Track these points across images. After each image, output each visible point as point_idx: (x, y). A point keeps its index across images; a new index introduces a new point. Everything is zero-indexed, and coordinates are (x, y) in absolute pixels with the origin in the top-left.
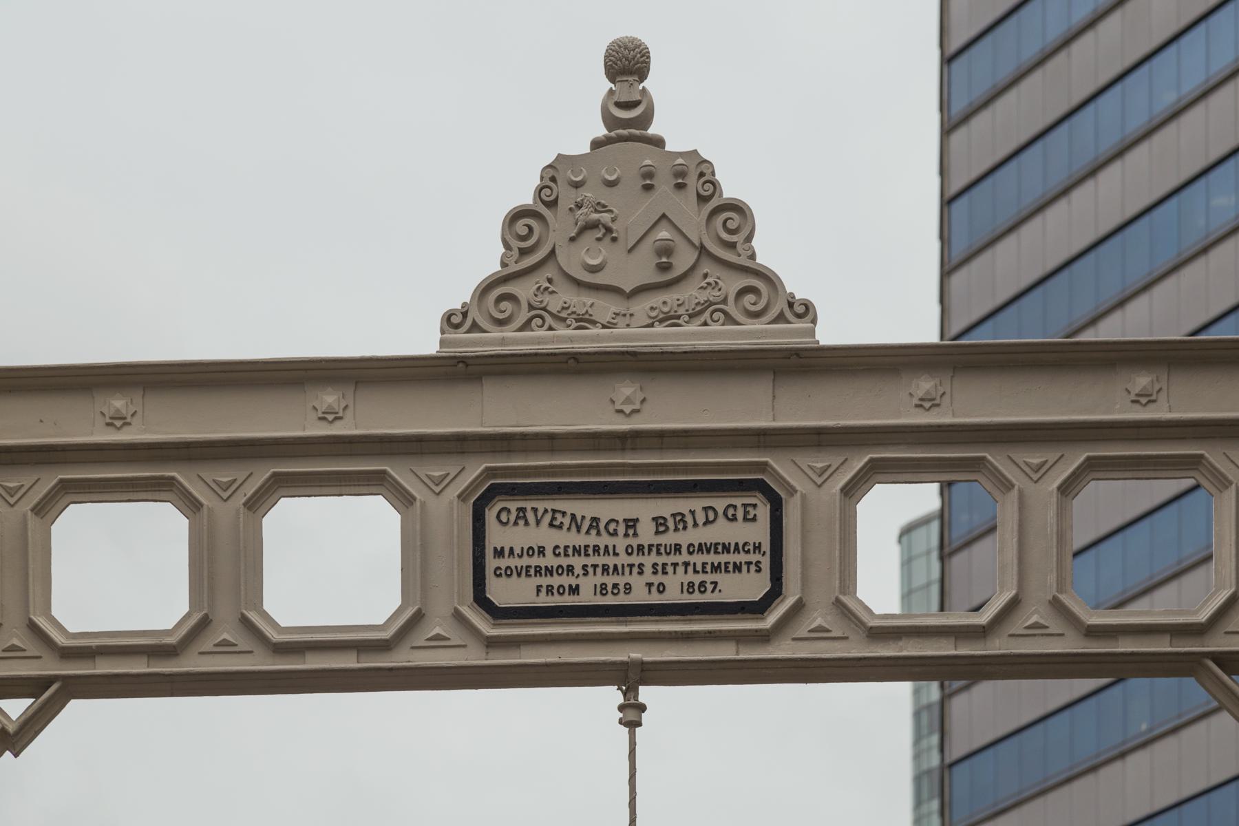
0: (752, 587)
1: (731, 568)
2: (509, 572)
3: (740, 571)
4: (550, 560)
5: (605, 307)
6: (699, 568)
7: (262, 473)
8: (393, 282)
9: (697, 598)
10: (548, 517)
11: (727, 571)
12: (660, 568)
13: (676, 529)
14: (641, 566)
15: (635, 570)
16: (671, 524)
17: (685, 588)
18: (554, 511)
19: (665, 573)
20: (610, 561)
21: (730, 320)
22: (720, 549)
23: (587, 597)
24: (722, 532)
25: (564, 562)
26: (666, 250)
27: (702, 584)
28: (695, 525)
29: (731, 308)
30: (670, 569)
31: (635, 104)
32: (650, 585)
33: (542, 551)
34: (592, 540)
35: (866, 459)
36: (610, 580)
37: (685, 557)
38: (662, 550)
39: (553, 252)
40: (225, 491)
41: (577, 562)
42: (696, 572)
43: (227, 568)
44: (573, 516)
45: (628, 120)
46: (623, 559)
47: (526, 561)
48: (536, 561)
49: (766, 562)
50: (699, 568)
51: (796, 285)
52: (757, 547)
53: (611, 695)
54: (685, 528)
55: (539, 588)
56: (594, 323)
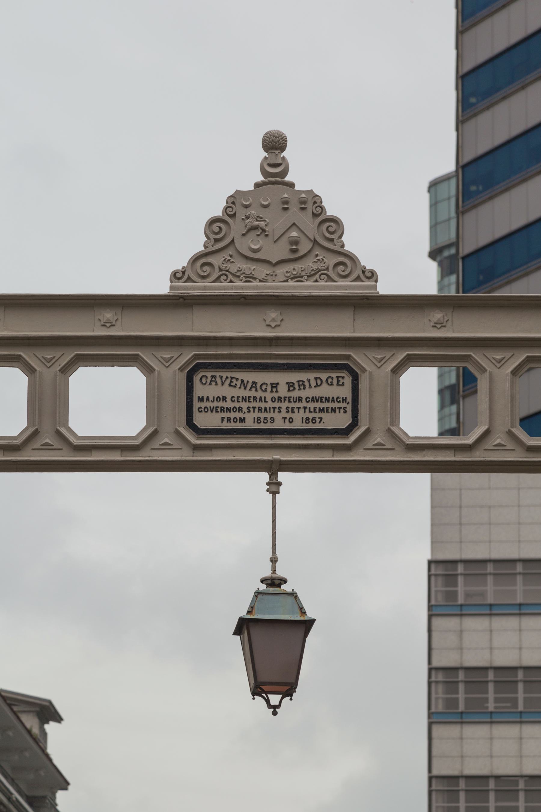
0: (342, 420)
1: (330, 410)
2: (206, 410)
3: (335, 412)
4: (229, 404)
5: (261, 271)
6: (312, 410)
7: (69, 354)
9: (311, 426)
11: (327, 412)
12: (290, 410)
13: (300, 389)
14: (280, 408)
15: (277, 410)
16: (296, 386)
17: (304, 420)
18: (232, 378)
19: (293, 412)
20: (263, 405)
22: (324, 400)
23: (250, 424)
24: (325, 391)
25: (237, 405)
26: (295, 242)
27: (314, 418)
28: (310, 387)
29: (331, 273)
30: (296, 410)
31: (279, 165)
32: (285, 418)
33: (224, 399)
34: (253, 393)
35: (405, 354)
36: (262, 415)
37: (304, 404)
38: (292, 400)
39: (233, 241)
40: (49, 363)
41: (244, 405)
42: (310, 412)
43: (48, 404)
44: (242, 381)
45: (275, 172)
46: (270, 404)
47: (215, 404)
48: (221, 404)
49: (349, 408)
50: (312, 410)
52: (345, 400)
53: (264, 477)
54: (304, 388)
55: (223, 419)
56: (255, 279)
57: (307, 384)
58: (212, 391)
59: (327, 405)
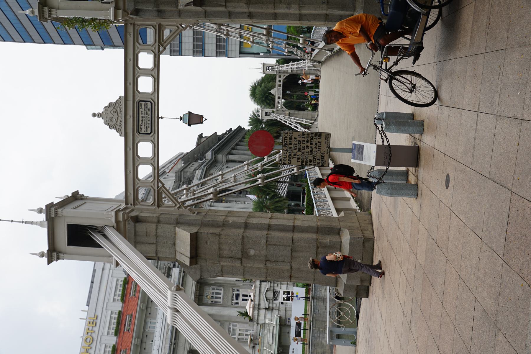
0: (149, 104)
5: (119, 119)
7: (136, 157)
8: (117, 141)
23: (150, 122)
24: (143, 107)
40: (138, 161)
45: (100, 115)
51: (118, 98)
53: (160, 119)
59: (146, 107)
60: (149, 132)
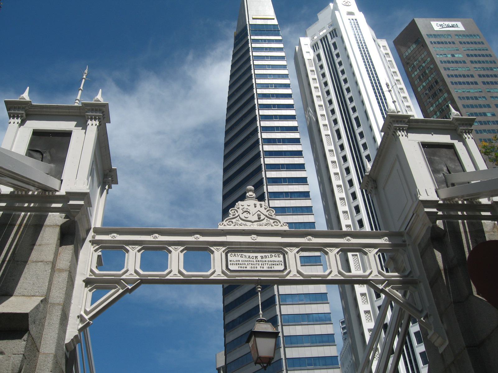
0: (282, 268)
3: (278, 265)
4: (241, 262)
9: (270, 269)
10: (240, 255)
11: (276, 265)
13: (265, 258)
14: (259, 264)
15: (258, 265)
18: (241, 255)
19: (263, 265)
20: (253, 263)
21: (272, 226)
23: (248, 269)
24: (274, 259)
28: (269, 257)
30: (264, 264)
32: (261, 267)
35: (300, 248)
39: (239, 215)
41: (246, 263)
46: (255, 263)
49: (283, 264)
52: (281, 261)
54: (267, 258)
55: (239, 267)
57: (267, 256)
58: (235, 259)
60: (231, 267)
